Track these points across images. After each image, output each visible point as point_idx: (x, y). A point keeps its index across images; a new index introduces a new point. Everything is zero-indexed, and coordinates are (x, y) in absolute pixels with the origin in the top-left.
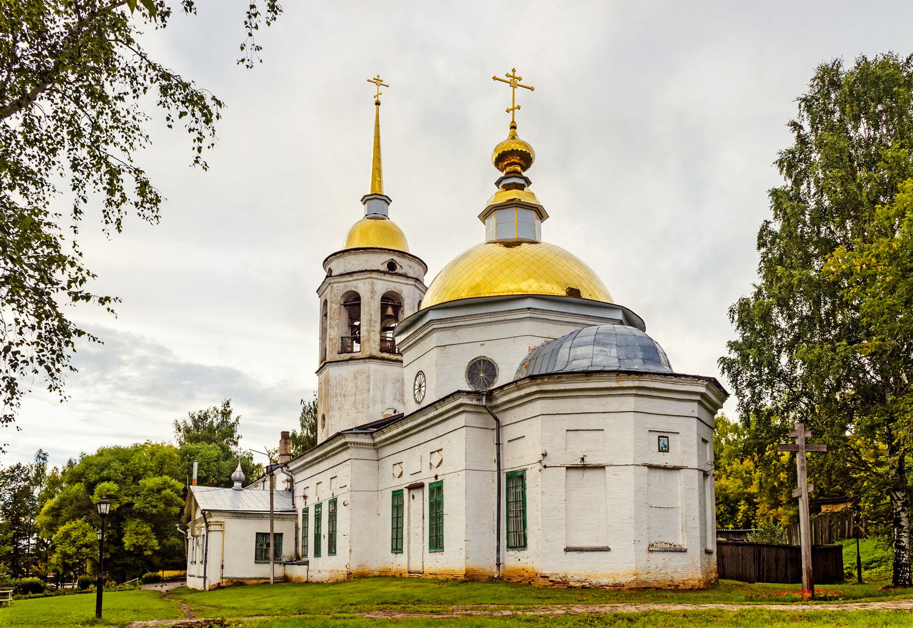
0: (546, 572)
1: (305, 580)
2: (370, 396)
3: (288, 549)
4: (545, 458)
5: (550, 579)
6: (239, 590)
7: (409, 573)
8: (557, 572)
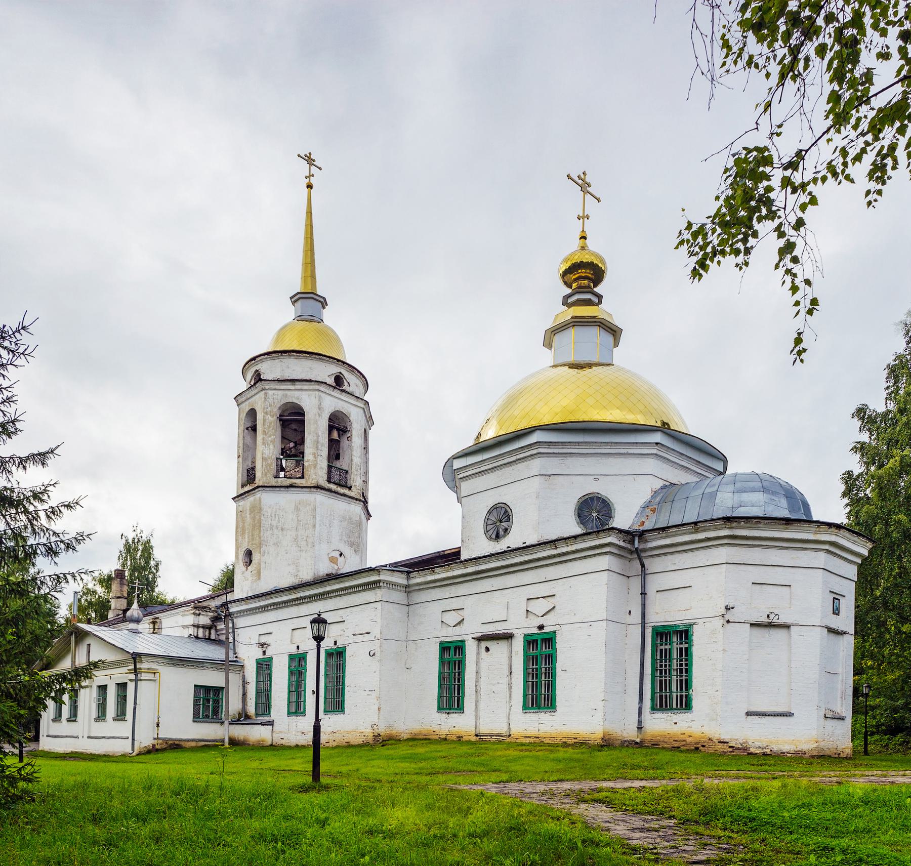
0: (725, 737)
1: (270, 743)
2: (316, 532)
3: (233, 704)
4: (729, 612)
5: (730, 745)
6: (170, 755)
7: (477, 735)
8: (736, 738)
